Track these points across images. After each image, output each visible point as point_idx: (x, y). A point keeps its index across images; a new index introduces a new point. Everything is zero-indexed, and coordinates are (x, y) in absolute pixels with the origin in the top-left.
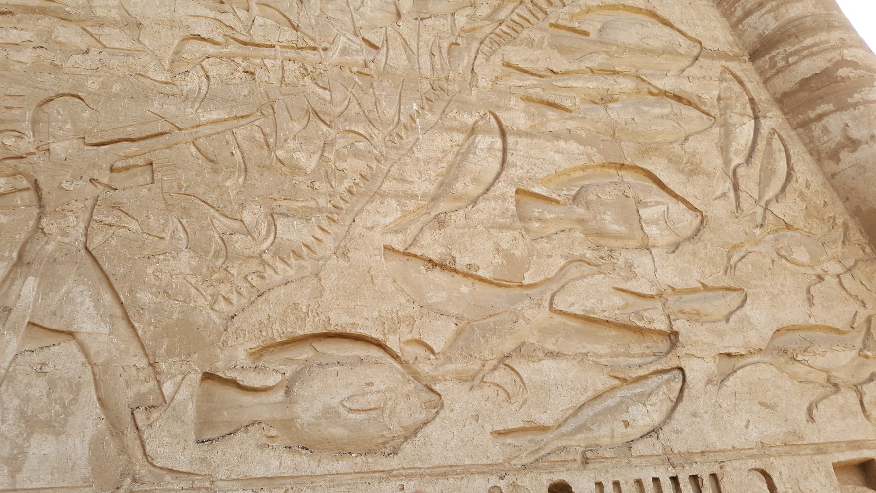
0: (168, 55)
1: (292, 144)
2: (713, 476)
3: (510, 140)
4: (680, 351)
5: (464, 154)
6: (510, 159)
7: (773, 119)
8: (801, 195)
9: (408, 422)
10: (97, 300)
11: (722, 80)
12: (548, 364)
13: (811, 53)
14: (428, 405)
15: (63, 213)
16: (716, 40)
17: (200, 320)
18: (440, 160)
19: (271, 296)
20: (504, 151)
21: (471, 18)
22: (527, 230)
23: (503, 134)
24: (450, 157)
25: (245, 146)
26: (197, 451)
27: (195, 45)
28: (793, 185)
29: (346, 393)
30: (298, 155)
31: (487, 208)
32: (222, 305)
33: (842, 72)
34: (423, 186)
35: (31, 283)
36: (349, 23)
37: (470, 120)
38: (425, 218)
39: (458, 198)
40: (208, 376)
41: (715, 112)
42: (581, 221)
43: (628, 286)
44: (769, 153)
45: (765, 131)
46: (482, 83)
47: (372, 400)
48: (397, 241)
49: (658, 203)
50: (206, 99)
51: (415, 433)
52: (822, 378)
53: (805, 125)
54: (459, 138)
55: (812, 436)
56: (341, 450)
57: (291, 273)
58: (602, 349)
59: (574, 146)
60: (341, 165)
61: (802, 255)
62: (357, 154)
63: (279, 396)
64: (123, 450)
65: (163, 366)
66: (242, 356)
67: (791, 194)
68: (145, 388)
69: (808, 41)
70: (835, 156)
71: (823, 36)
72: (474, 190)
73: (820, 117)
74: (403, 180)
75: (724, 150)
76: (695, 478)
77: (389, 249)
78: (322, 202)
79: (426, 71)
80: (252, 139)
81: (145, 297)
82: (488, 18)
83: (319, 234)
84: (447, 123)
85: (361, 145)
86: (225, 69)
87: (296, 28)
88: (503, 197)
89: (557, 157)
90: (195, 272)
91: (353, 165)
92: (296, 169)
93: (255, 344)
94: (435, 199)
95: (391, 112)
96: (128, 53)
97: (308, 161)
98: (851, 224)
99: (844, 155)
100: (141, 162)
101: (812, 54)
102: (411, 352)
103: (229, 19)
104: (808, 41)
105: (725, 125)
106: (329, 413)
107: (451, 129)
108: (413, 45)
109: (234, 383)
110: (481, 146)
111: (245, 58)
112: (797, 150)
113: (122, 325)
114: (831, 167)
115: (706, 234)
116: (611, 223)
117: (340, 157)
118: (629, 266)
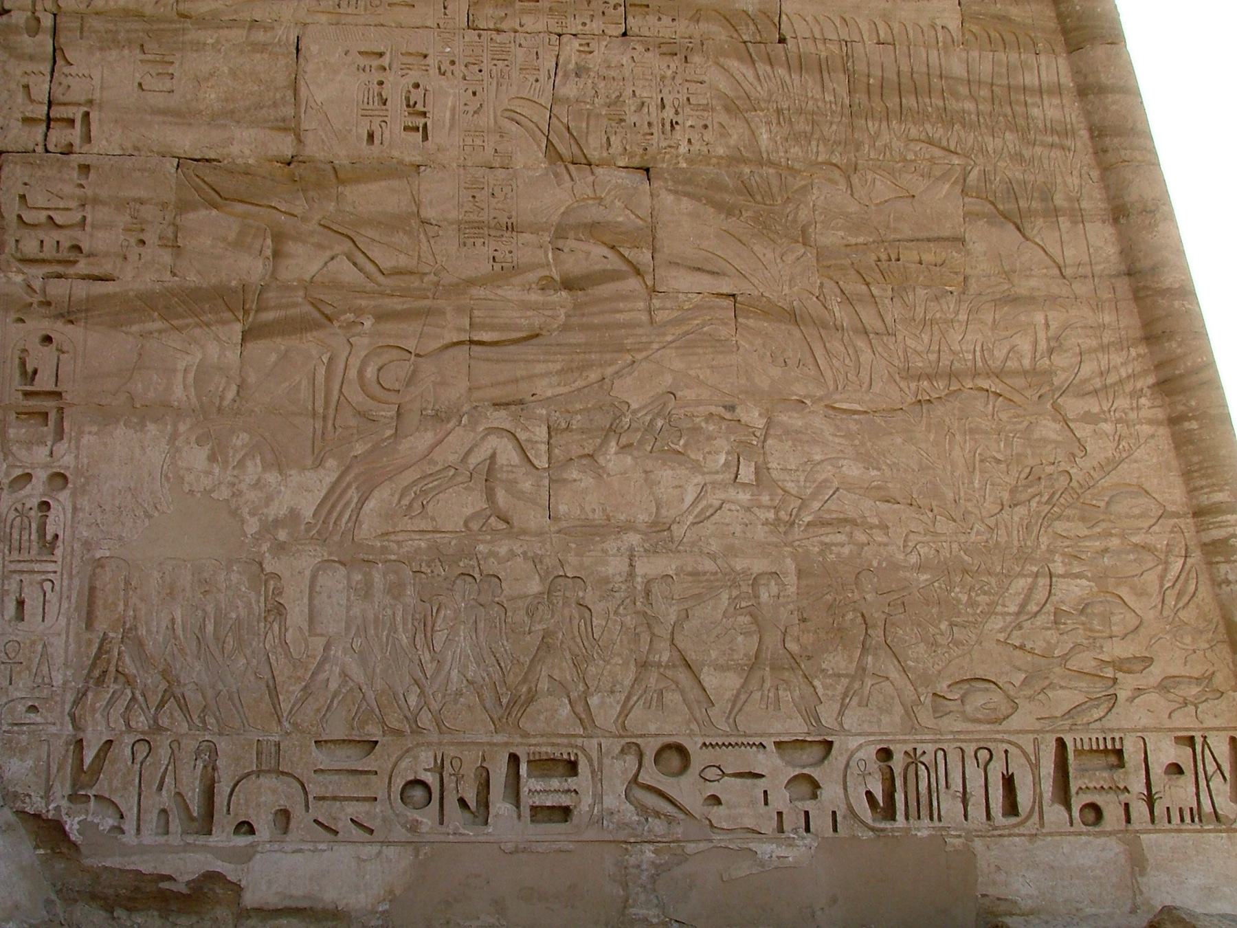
0: (901, 544)
1: (957, 590)
2: (1121, 738)
3: (1054, 579)
4: (1117, 687)
5: (1031, 589)
6: (1053, 591)
7: (1196, 557)
8: (1198, 606)
9: (1005, 713)
10: (893, 664)
11: (1172, 532)
12: (1060, 692)
13: (1220, 526)
14: (1012, 707)
15: (875, 626)
16: (1174, 503)
17: (930, 673)
18: (1020, 594)
19: (953, 662)
20: (1051, 586)
21: (1038, 503)
22: (1058, 629)
23: (1051, 576)
24: (1025, 591)
25: (938, 591)
26: (934, 721)
27: (912, 536)
28: (1195, 599)
29: (983, 702)
30: (960, 595)
31: (1040, 620)
32: (936, 666)
33: (1233, 541)
34: (1013, 608)
35: (870, 658)
36: (979, 515)
37: (1035, 569)
38: (1013, 624)
39: (1028, 613)
40: (934, 694)
41: (1162, 557)
42: (1083, 624)
43: (1099, 657)
44: (1187, 580)
45: (1188, 566)
46: (1042, 546)
47: (992, 706)
48: (1002, 637)
49: (1121, 613)
50: (920, 568)
51: (1008, 717)
52: (1181, 700)
53: (1210, 563)
54: (1030, 580)
55: (1168, 724)
56: (979, 721)
57: (960, 652)
58: (1083, 684)
59: (1084, 582)
60: (978, 599)
61: (1188, 640)
62: (985, 593)
63: (959, 701)
64: (910, 719)
65: (920, 690)
66: (945, 686)
67: (1191, 605)
68: (913, 698)
69: (1219, 519)
70: (1219, 585)
71: (1229, 517)
72: (1035, 609)
73: (1218, 563)
74: (1004, 606)
75: (1162, 578)
76: (1113, 739)
77: (998, 640)
78: (971, 619)
79: (1016, 543)
80: (940, 588)
81: (910, 663)
82: (1046, 503)
83: (970, 634)
84: (1025, 573)
85: (986, 588)
86: (926, 549)
87: (954, 521)
88: (1048, 613)
89: (1076, 589)
90: (926, 651)
91: (982, 599)
92: (959, 601)
93: (949, 683)
94: (1018, 614)
95: (998, 569)
96: (886, 545)
97: (964, 598)
98: (1221, 623)
99: (1224, 586)
100: (899, 602)
101: (1220, 527)
102: (1005, 687)
103: (924, 518)
104: (1219, 519)
105: (1166, 563)
106: (977, 709)
107: (1025, 576)
108: (1009, 524)
109: (944, 697)
110: (1041, 584)
111: (934, 542)
112: (1204, 578)
113: (902, 673)
114: (1218, 591)
115: (1142, 630)
116: (1096, 625)
117: (977, 595)
118: (1102, 647)
